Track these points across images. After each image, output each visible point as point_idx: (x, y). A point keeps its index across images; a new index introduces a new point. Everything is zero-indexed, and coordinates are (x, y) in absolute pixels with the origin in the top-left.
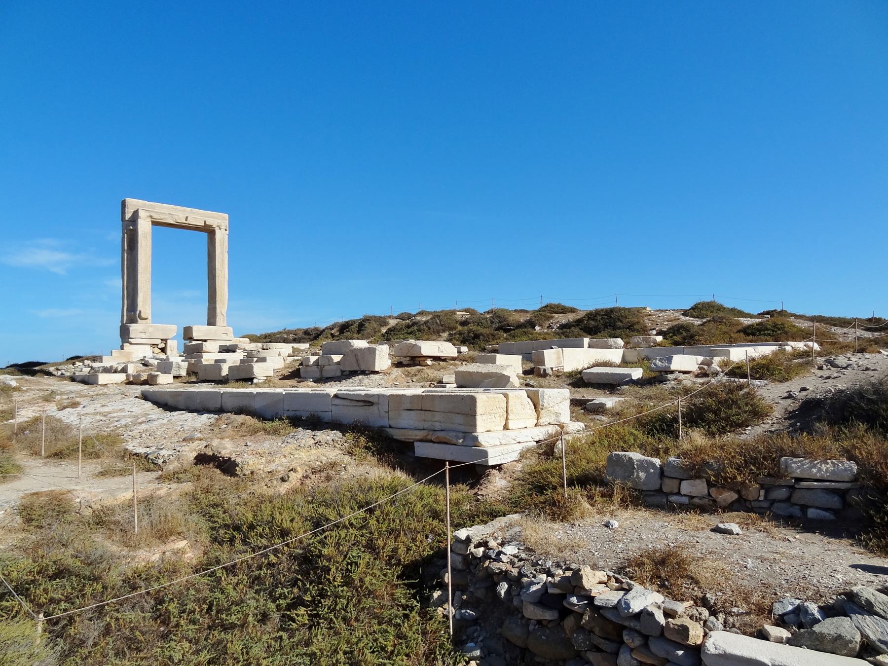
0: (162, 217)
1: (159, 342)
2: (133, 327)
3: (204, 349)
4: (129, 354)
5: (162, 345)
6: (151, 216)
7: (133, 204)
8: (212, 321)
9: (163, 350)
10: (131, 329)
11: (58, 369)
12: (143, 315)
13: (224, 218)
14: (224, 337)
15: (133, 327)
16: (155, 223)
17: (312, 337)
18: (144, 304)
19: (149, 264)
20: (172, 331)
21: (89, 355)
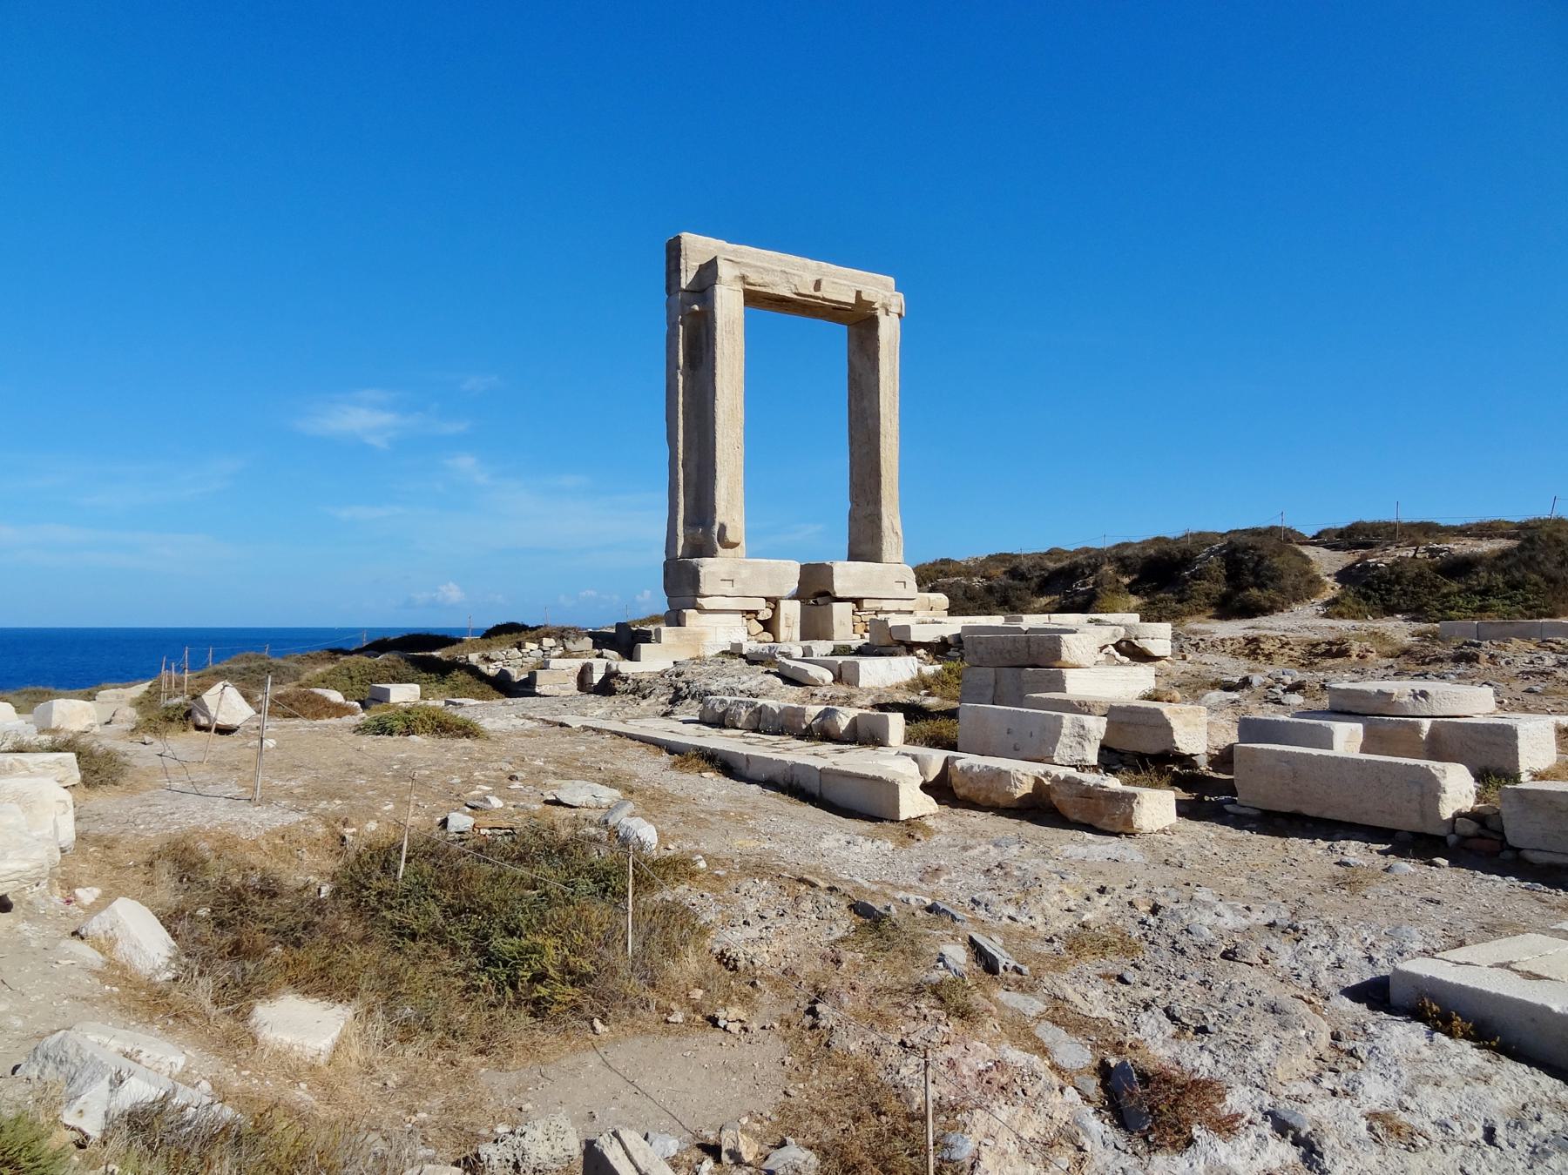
0: (767, 279)
1: (760, 605)
2: (711, 569)
4: (697, 638)
5: (766, 614)
6: (743, 278)
7: (697, 248)
8: (865, 546)
9: (769, 626)
10: (702, 571)
11: (488, 660)
12: (731, 536)
13: (886, 286)
14: (899, 591)
16: (755, 299)
17: (1033, 585)
18: (730, 506)
19: (740, 401)
20: (787, 577)
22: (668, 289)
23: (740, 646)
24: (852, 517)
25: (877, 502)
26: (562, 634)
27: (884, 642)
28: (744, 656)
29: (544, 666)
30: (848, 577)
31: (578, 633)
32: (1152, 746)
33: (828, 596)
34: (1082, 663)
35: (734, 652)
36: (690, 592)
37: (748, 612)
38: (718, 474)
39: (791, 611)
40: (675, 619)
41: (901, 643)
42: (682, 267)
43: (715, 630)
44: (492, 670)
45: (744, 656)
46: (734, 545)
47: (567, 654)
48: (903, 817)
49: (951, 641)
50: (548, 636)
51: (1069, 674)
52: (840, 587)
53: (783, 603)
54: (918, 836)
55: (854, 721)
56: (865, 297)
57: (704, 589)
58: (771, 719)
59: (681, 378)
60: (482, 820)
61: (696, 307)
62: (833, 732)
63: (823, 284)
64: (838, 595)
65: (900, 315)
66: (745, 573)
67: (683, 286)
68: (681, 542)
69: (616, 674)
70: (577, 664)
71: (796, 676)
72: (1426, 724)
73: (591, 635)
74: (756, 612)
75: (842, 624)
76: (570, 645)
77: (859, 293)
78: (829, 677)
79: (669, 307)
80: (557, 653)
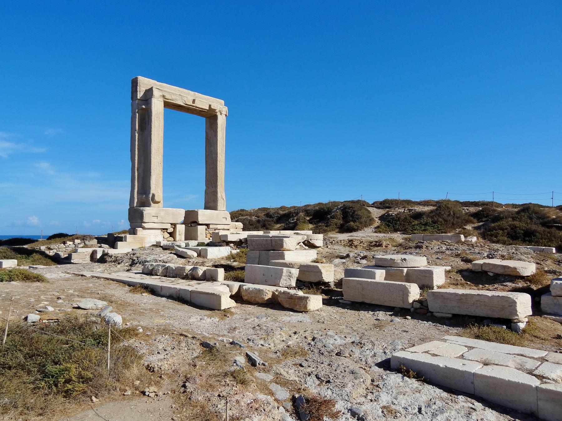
0: (174, 97)
2: (148, 211)
3: (285, 246)
4: (142, 240)
5: (171, 230)
6: (164, 96)
7: (145, 83)
8: (211, 203)
9: (172, 234)
10: (145, 213)
11: (49, 249)
12: (157, 199)
14: (224, 221)
15: (148, 211)
17: (274, 220)
19: (161, 145)
20: (180, 215)
21: (81, 233)
22: (132, 98)
23: (160, 242)
24: (206, 193)
25: (216, 187)
26: (83, 238)
27: (218, 241)
28: (161, 247)
29: (75, 251)
30: (204, 215)
31: (91, 238)
32: (314, 279)
33: (196, 223)
34: (291, 249)
35: (158, 245)
36: (139, 221)
37: (164, 229)
38: (152, 174)
39: (181, 229)
40: (133, 232)
41: (224, 241)
42: (138, 90)
43: (149, 236)
44: (51, 253)
45: (161, 247)
46: (158, 202)
47: (86, 246)
48: (222, 308)
49: (243, 241)
50: (77, 238)
51: (286, 253)
52: (201, 220)
53: (178, 227)
54: (228, 315)
55: (205, 272)
56: (212, 107)
57: (145, 220)
58: (171, 272)
59: (137, 135)
60: (43, 316)
61: (144, 107)
62: (196, 276)
63: (196, 101)
64: (200, 223)
65: (226, 115)
66: (162, 214)
67: (139, 98)
68: (136, 201)
69: (107, 254)
70: (90, 250)
71: (182, 255)
72: (405, 270)
73: (96, 238)
74: (167, 229)
75: (201, 234)
76: (87, 242)
77: (210, 106)
78: (195, 255)
79: (132, 105)
80: (81, 246)
